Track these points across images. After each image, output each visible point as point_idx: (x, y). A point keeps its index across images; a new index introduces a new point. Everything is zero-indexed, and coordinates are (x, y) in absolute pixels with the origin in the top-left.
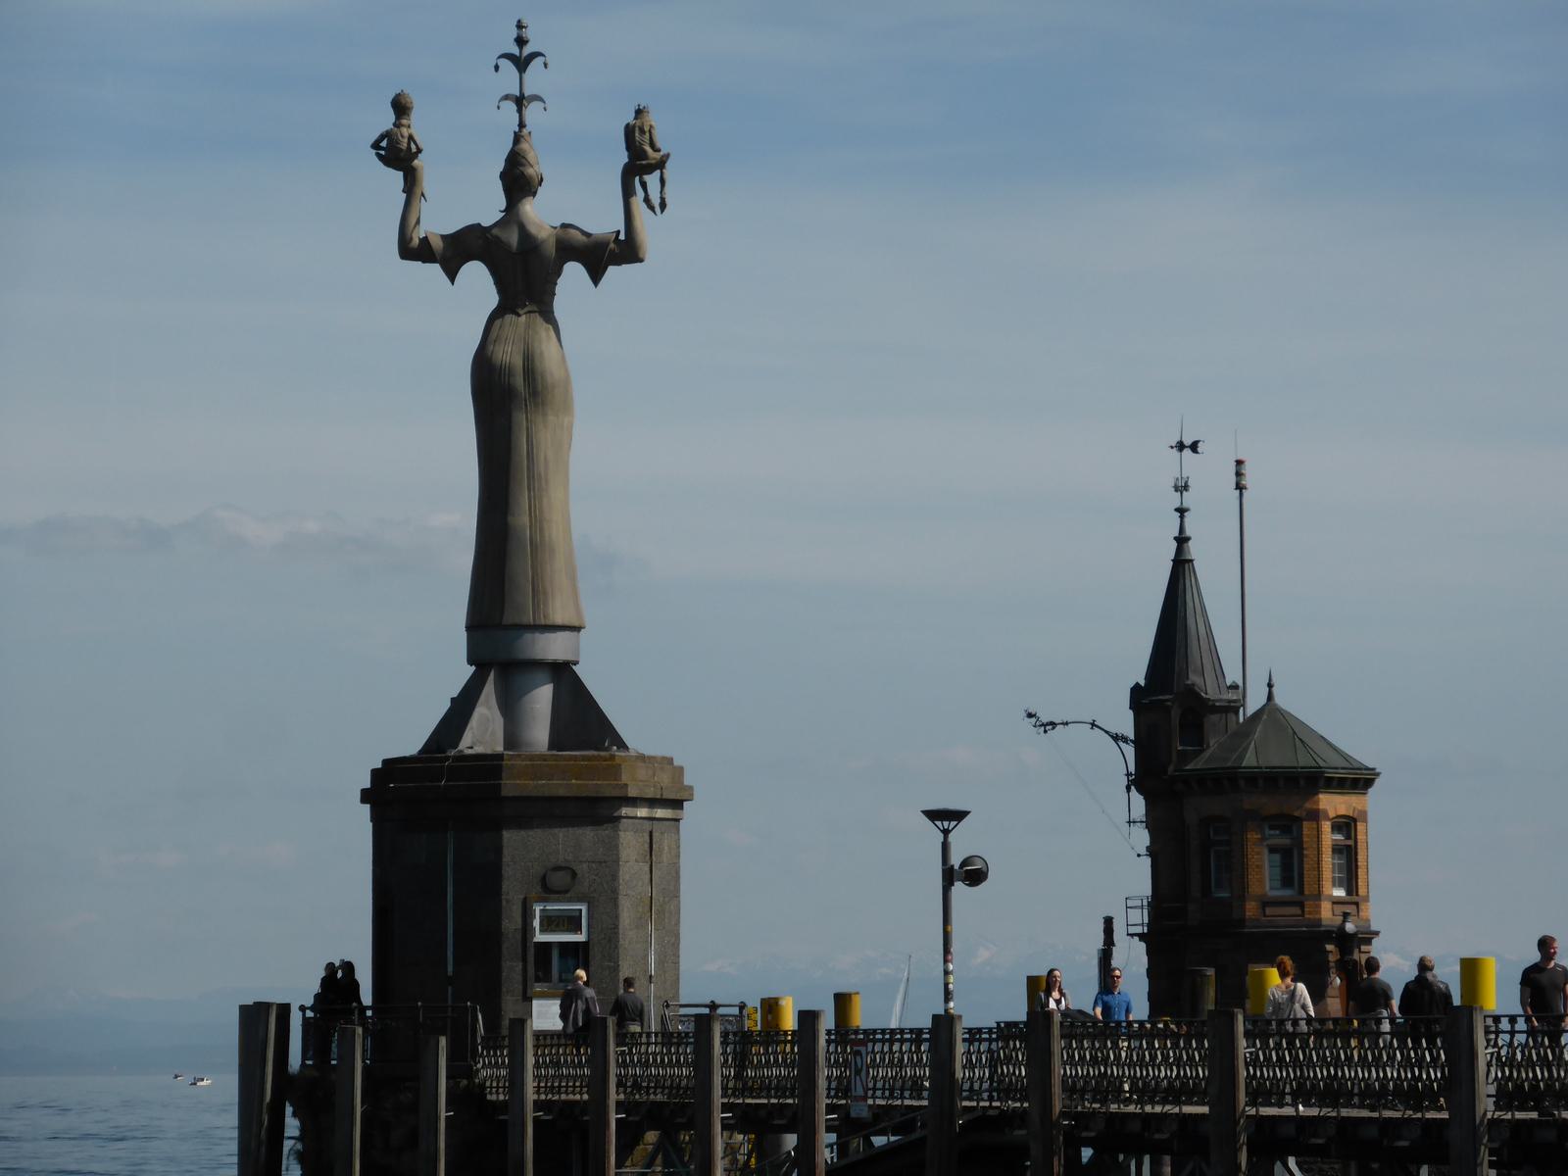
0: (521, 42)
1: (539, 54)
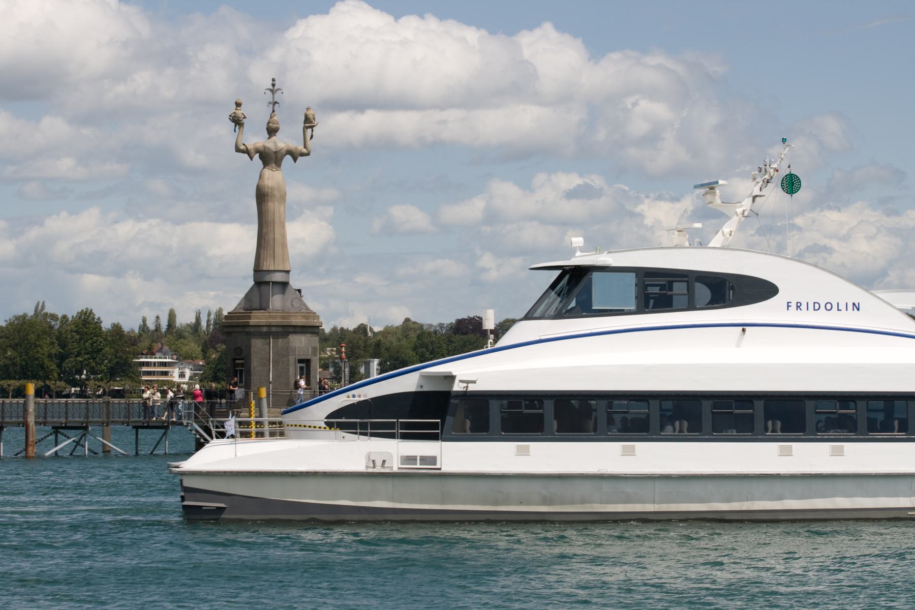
0: (273, 85)
1: (280, 89)
